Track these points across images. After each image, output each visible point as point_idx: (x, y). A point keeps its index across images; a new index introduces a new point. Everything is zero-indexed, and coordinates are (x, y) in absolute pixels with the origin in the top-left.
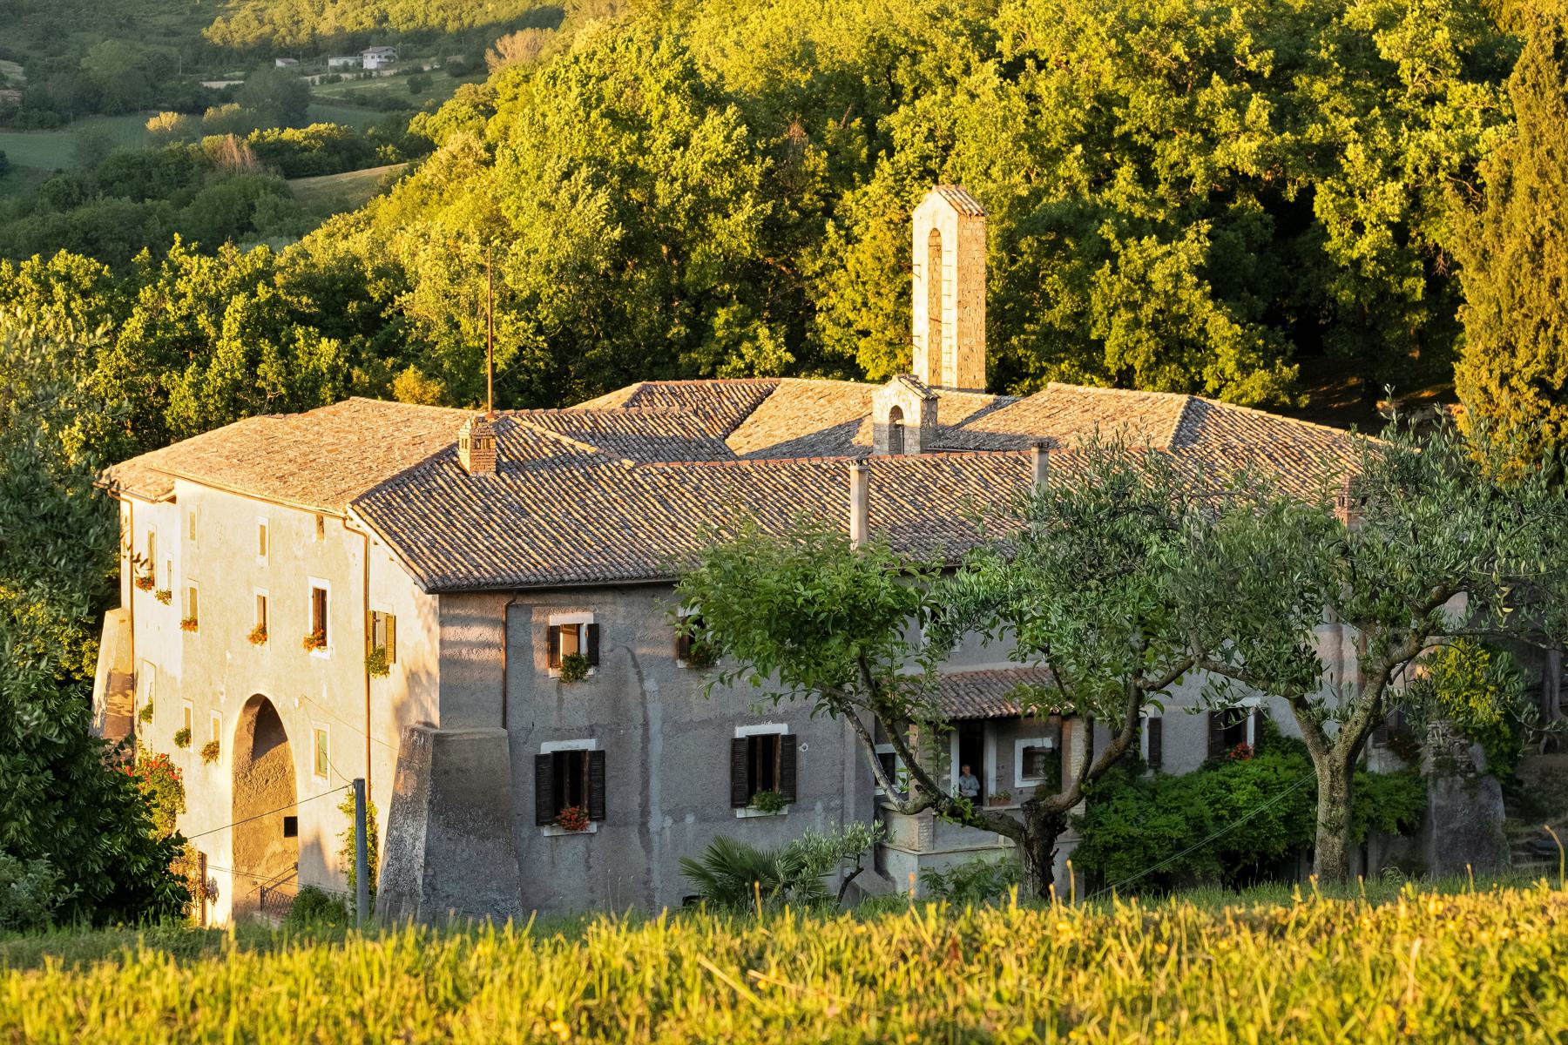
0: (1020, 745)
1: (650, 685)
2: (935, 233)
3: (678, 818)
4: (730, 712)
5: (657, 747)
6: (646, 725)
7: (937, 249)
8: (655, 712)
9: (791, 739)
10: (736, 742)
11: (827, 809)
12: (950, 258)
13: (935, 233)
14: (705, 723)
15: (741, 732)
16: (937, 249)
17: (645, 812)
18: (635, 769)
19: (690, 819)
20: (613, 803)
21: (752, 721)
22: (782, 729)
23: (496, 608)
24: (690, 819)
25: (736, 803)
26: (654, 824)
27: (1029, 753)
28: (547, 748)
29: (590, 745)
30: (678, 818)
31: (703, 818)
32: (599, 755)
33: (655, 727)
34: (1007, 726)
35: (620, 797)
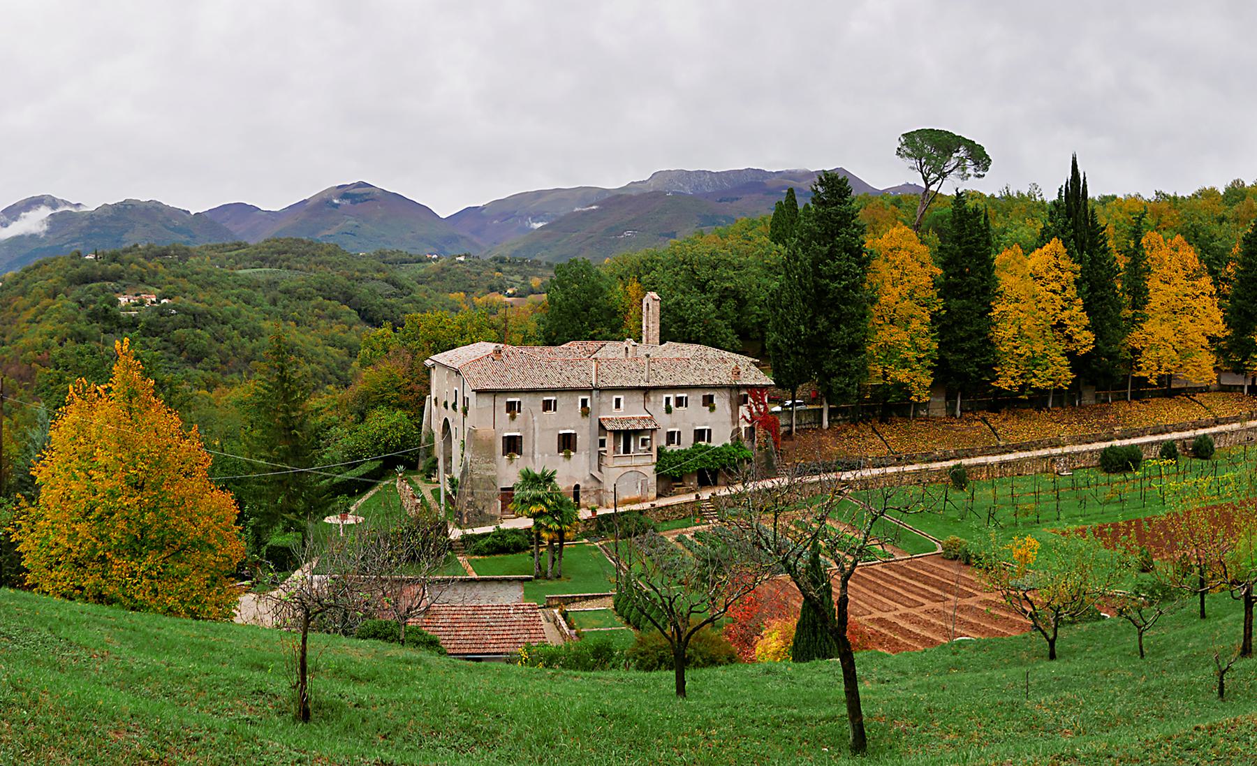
0: (641, 438)
1: (535, 418)
2: (648, 304)
3: (543, 455)
4: (558, 426)
5: (537, 436)
6: (534, 429)
7: (648, 309)
8: (537, 425)
9: (575, 434)
10: (559, 435)
11: (586, 454)
12: (650, 311)
13: (648, 304)
14: (551, 429)
15: (561, 432)
16: (648, 309)
17: (533, 453)
18: (531, 440)
19: (546, 455)
21: (565, 429)
22: (573, 432)
23: (492, 395)
24: (546, 455)
25: (559, 452)
26: (536, 456)
27: (644, 441)
28: (506, 435)
29: (518, 434)
30: (543, 455)
31: (550, 455)
32: (521, 437)
33: (536, 430)
34: (637, 432)
35: (526, 448)
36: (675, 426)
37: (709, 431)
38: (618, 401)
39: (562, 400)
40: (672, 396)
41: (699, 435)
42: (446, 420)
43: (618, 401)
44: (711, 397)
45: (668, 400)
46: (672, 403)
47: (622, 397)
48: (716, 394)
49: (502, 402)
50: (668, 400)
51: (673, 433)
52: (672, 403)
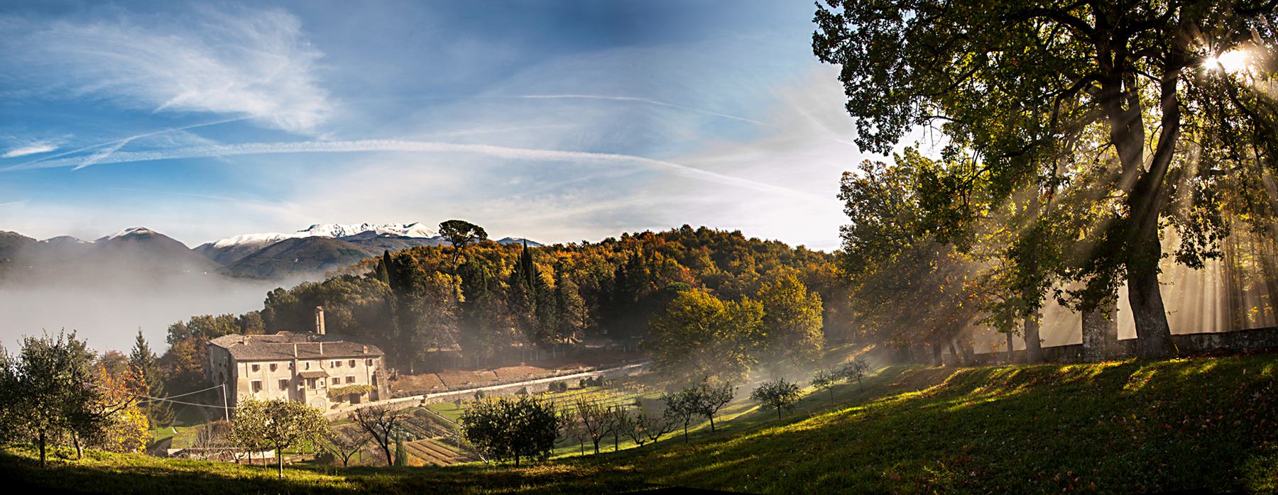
3: (273, 389)
8: (268, 376)
20: (263, 388)
26: (269, 390)
35: (263, 386)
36: (337, 375)
37: (354, 377)
38: (307, 364)
39: (279, 364)
40: (334, 361)
41: (350, 379)
42: (221, 373)
43: (307, 364)
44: (354, 361)
45: (332, 363)
46: (334, 364)
47: (309, 362)
48: (356, 360)
49: (250, 365)
50: (332, 363)
51: (336, 379)
52: (334, 364)
